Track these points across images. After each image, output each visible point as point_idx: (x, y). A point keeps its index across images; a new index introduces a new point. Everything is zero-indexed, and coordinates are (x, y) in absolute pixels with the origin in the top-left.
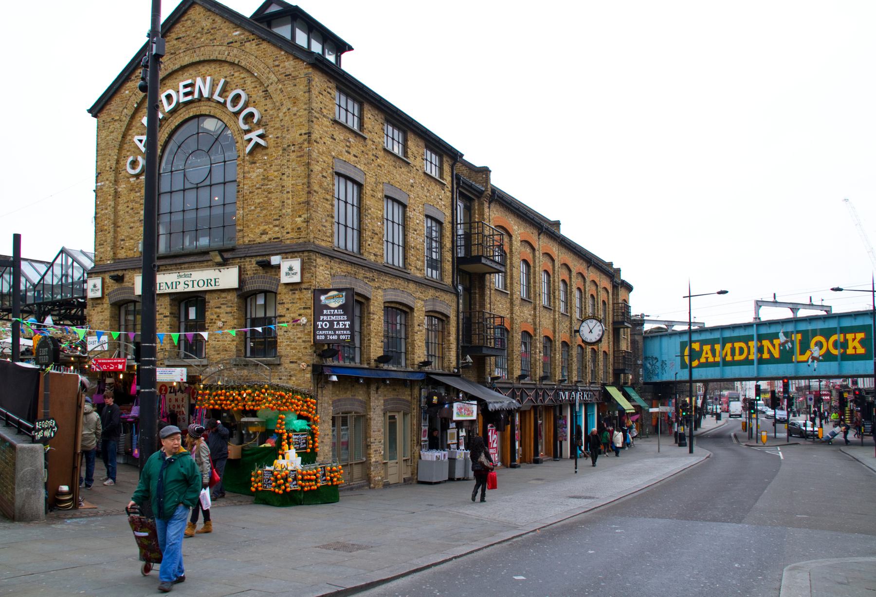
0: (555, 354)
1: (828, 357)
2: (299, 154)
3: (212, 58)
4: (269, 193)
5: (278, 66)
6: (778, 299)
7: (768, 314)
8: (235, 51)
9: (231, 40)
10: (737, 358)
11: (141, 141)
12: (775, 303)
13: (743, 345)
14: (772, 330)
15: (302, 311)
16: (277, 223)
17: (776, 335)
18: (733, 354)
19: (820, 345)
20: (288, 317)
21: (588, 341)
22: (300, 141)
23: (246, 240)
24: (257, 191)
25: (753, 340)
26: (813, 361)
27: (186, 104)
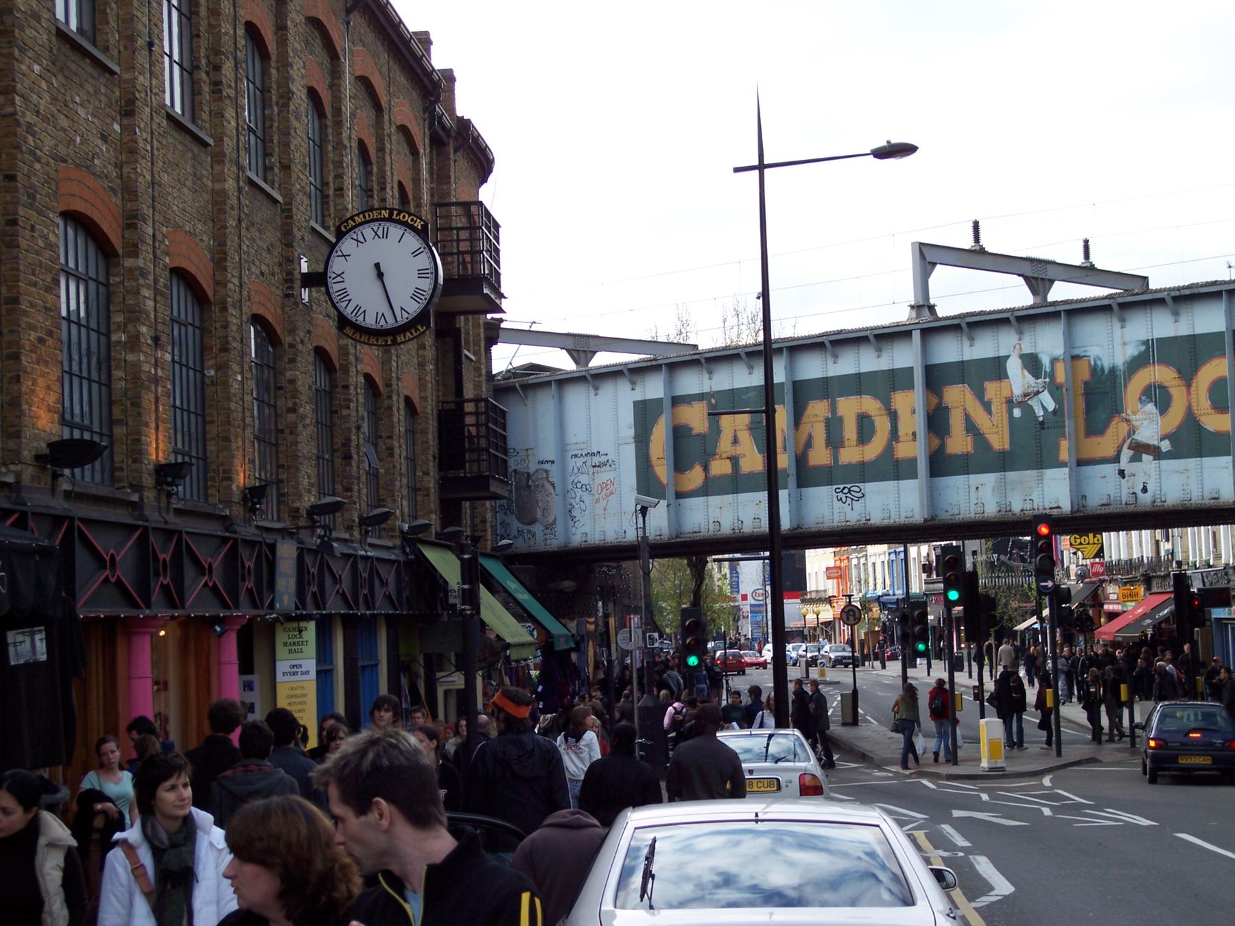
0: (222, 368)
1: (1192, 441)
6: (991, 244)
7: (958, 293)
10: (851, 454)
12: (977, 257)
13: (870, 405)
14: (983, 347)
17: (996, 368)
18: (834, 441)
19: (1159, 396)
21: (370, 321)
25: (910, 386)
26: (1136, 458)
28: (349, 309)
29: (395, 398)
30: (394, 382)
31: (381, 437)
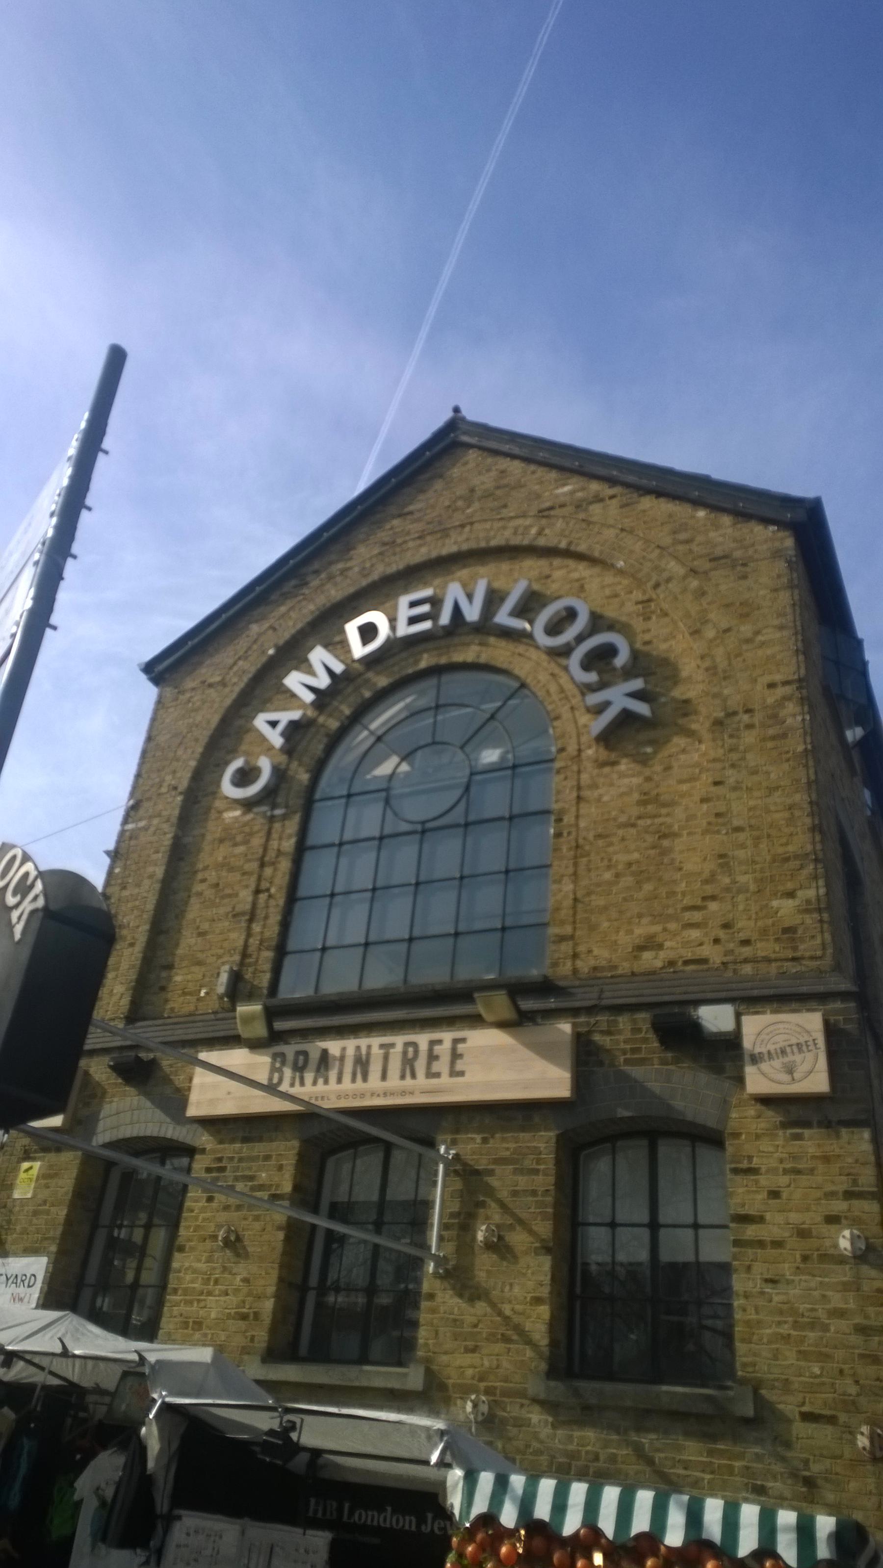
2: (771, 732)
3: (493, 543)
4: (664, 836)
5: (687, 542)
8: (560, 524)
9: (548, 504)
11: (273, 724)
15: (839, 1206)
16: (697, 916)
20: (776, 1225)
22: (771, 698)
23: (584, 966)
24: (620, 832)
27: (411, 641)
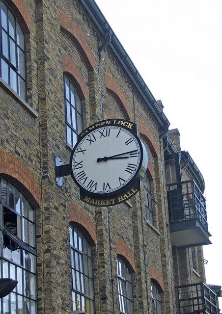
28: (86, 184)
29: (143, 274)
30: (142, 266)
31: (135, 297)
